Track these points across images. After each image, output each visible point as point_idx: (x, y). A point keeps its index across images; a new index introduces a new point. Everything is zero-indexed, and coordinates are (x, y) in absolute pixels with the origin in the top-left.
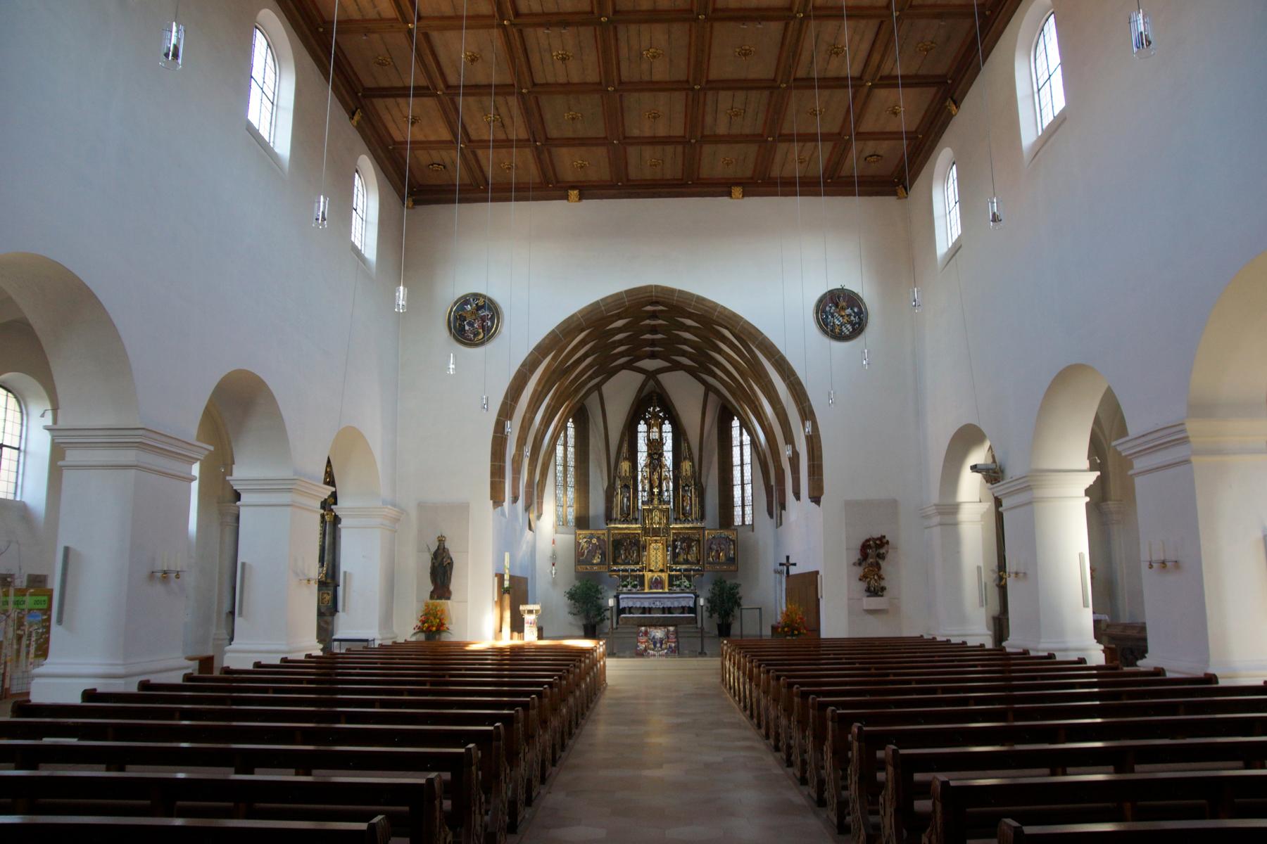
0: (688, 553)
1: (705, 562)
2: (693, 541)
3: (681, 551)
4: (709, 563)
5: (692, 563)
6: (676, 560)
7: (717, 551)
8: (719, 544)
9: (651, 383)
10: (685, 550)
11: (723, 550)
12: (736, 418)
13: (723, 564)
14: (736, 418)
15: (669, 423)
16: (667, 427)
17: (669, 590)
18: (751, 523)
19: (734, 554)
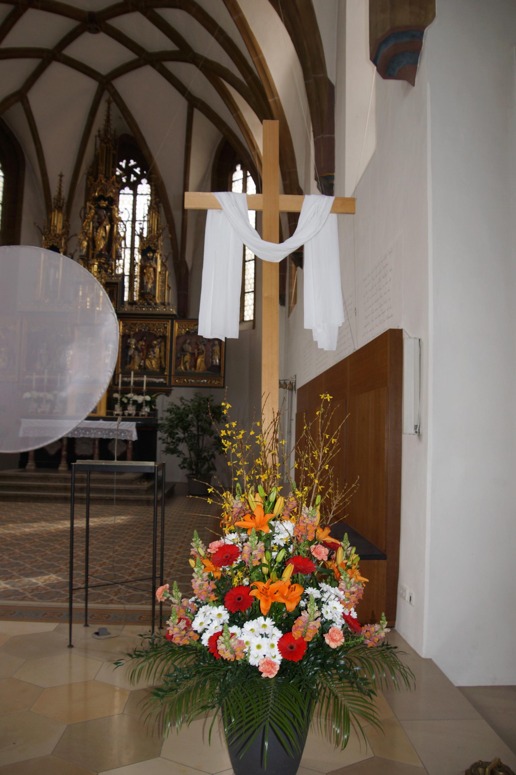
0: (146, 357)
1: (173, 373)
2: (156, 338)
3: (136, 353)
4: (180, 375)
5: (150, 373)
6: (128, 366)
7: (193, 354)
8: (197, 344)
9: (106, 96)
10: (143, 352)
11: (202, 352)
12: (238, 168)
13: (201, 376)
14: (238, 168)
15: (148, 183)
16: (144, 188)
17: (107, 414)
18: (252, 318)
19: (220, 360)
